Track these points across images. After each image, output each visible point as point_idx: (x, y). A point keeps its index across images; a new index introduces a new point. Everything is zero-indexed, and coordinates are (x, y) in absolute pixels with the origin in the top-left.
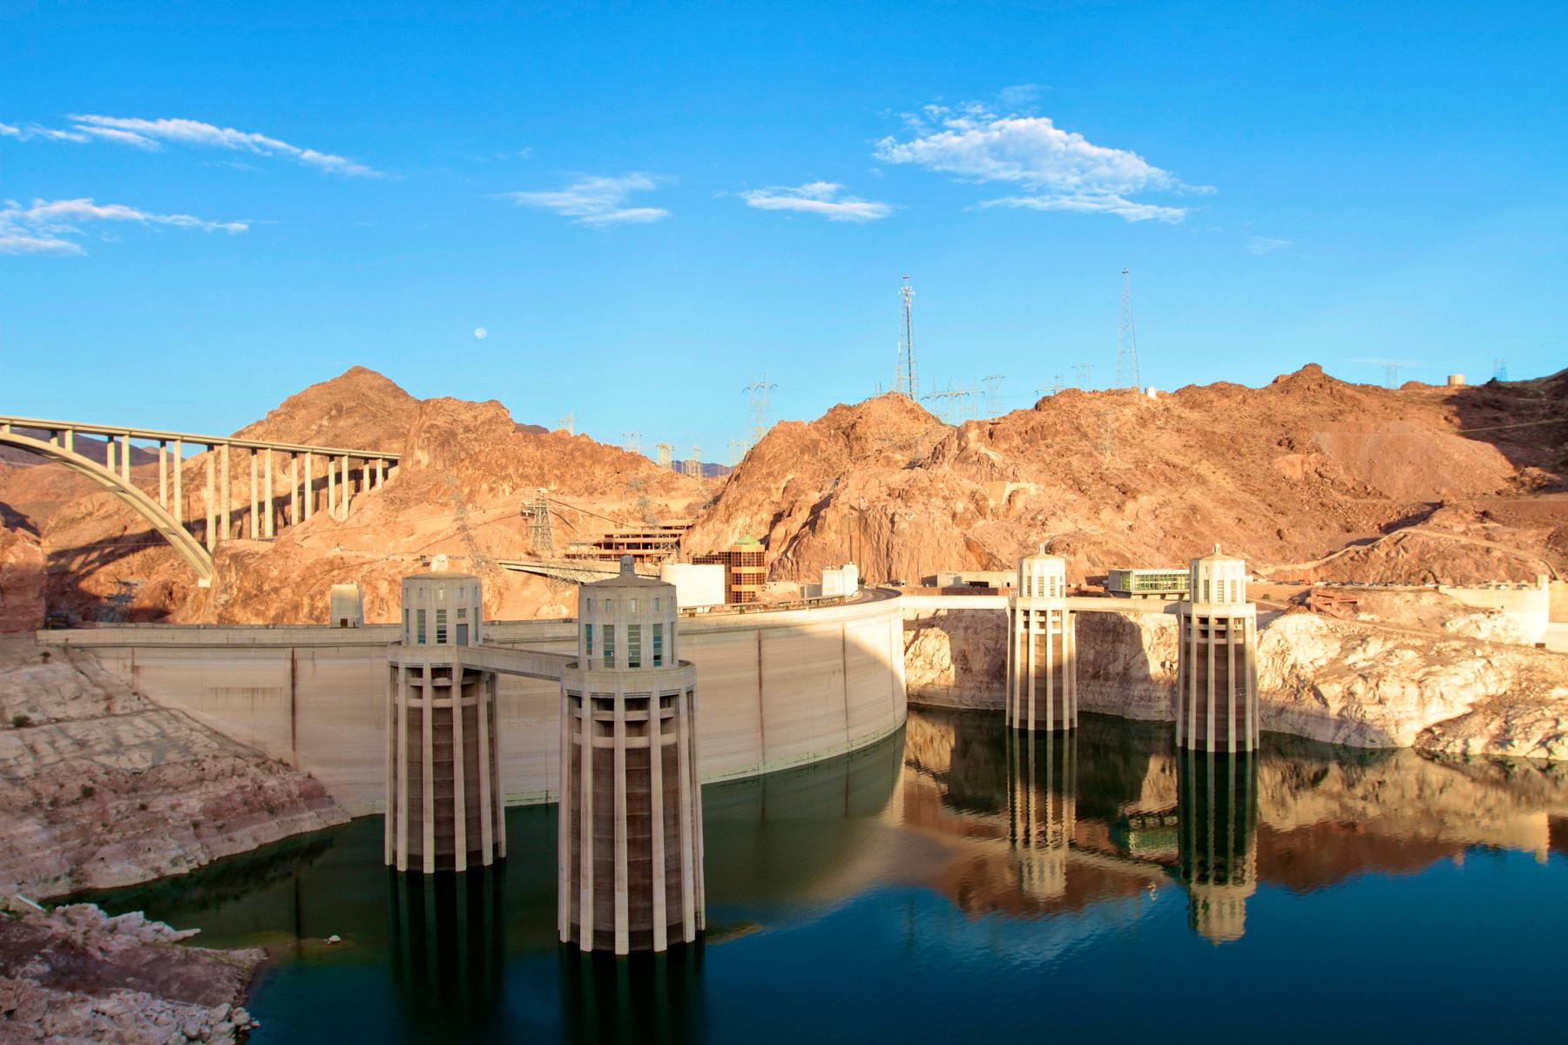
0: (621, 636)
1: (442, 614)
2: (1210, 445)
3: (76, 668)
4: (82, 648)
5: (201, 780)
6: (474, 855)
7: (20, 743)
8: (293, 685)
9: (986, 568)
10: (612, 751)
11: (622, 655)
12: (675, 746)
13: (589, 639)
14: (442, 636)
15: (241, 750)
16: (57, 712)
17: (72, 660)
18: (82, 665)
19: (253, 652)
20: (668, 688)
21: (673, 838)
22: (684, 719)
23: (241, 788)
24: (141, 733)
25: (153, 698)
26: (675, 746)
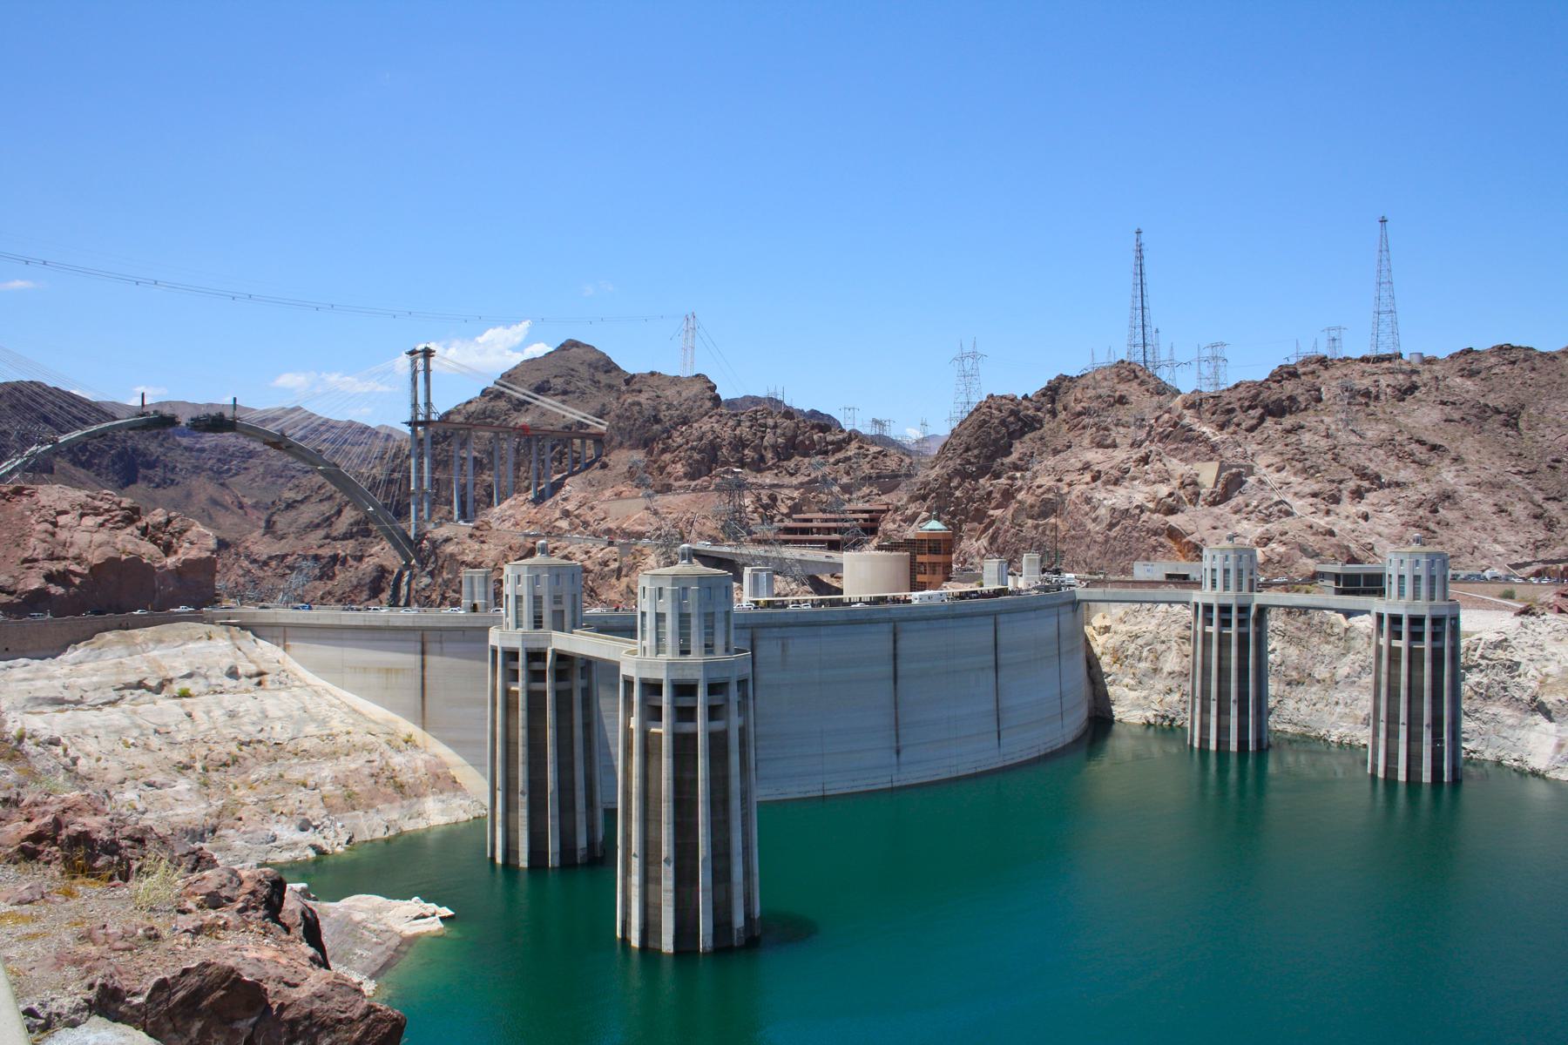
7: (181, 711)
17: (232, 638)
22: (734, 707)
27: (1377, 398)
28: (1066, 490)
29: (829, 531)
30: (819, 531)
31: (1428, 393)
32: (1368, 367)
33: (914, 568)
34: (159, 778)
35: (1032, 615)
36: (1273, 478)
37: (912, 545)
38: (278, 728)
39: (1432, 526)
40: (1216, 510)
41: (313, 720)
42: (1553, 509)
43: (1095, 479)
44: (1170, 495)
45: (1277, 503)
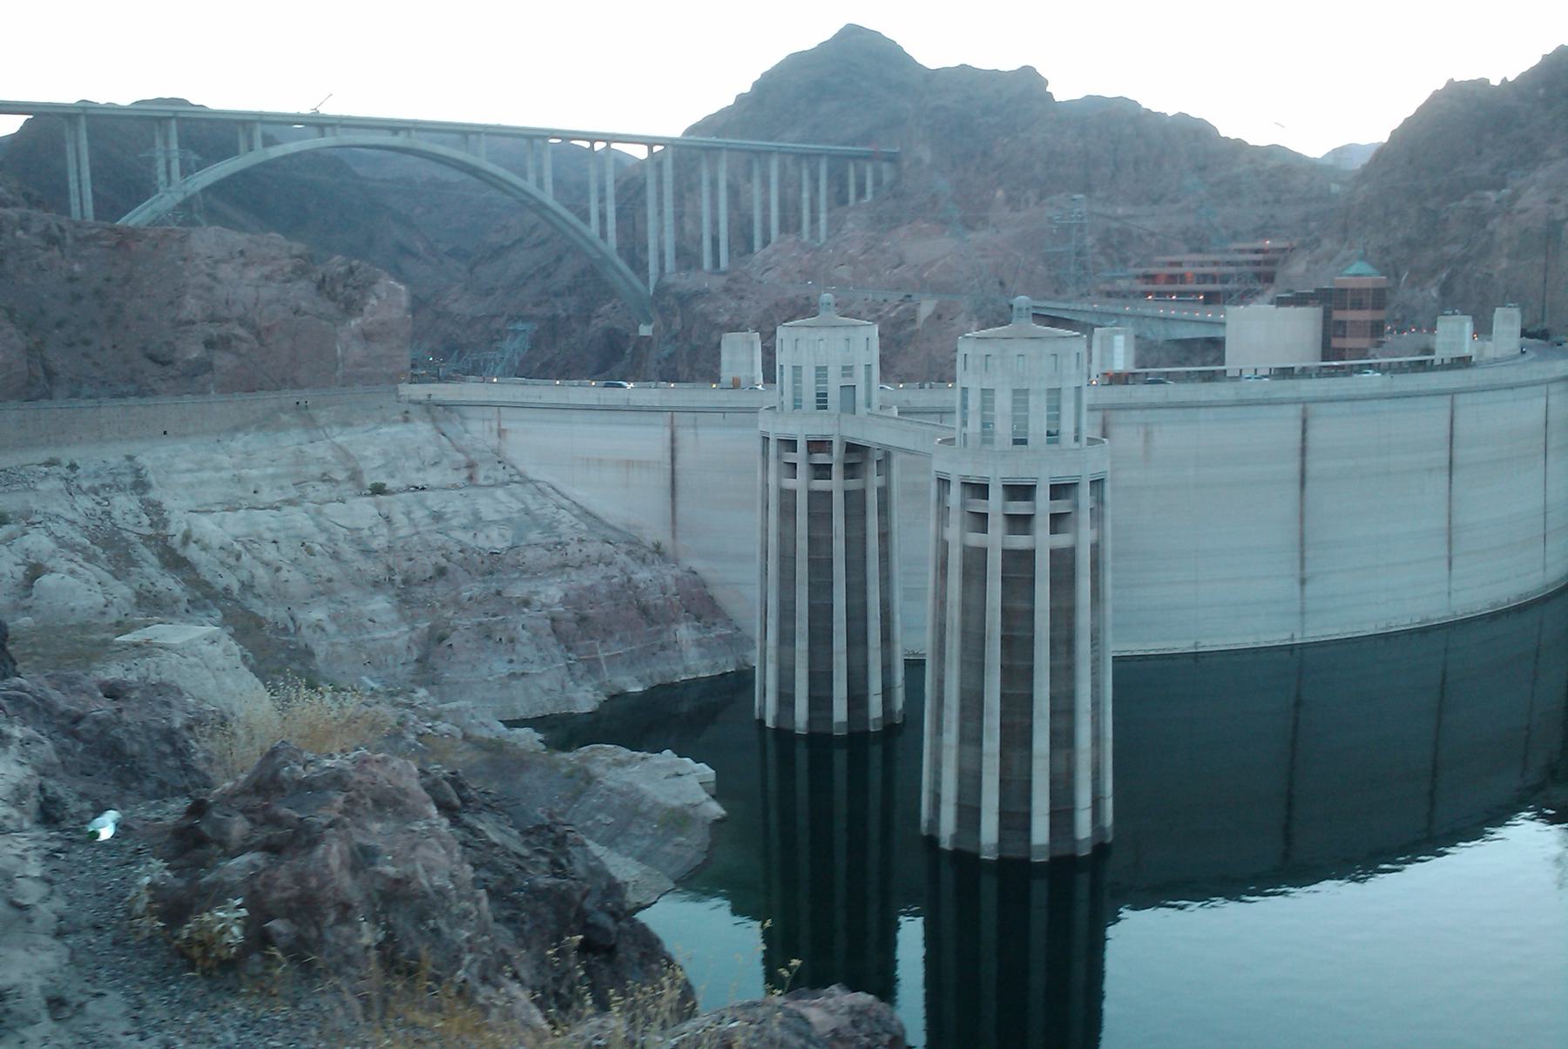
0: (1003, 402)
1: (821, 372)
3: (437, 428)
4: (446, 406)
5: (565, 566)
8: (673, 459)
11: (1003, 429)
13: (965, 406)
14: (822, 401)
15: (610, 533)
16: (418, 479)
17: (434, 420)
18: (444, 426)
20: (1062, 473)
22: (1085, 517)
23: (607, 578)
24: (502, 508)
25: (521, 468)
29: (1203, 278)
33: (1331, 330)
35: (1508, 394)
37: (1328, 298)
41: (539, 526)
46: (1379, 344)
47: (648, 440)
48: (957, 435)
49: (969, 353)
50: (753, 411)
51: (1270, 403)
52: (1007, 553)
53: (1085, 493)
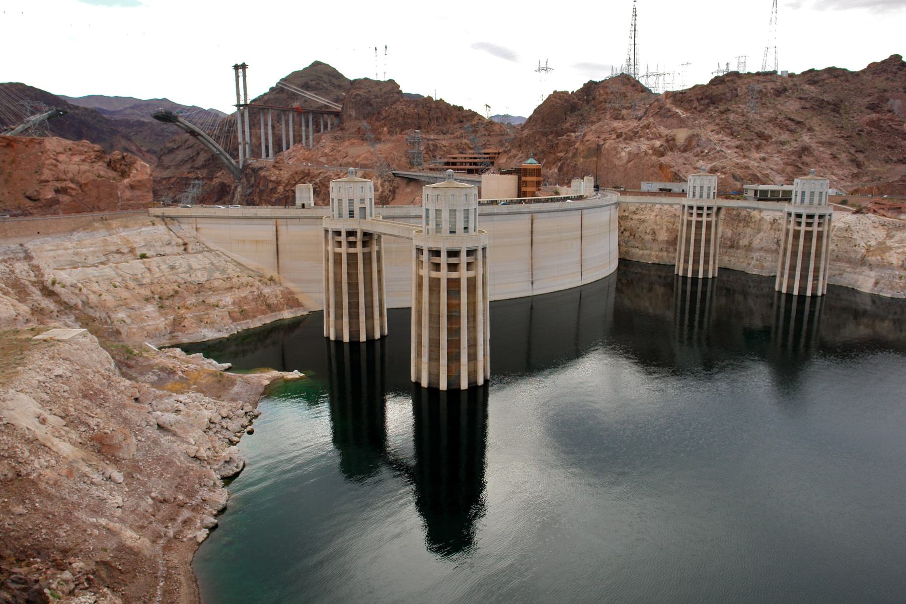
0: (445, 215)
1: (351, 201)
2: (819, 106)
6: (370, 331)
9: (670, 181)
10: (439, 279)
11: (446, 227)
12: (475, 278)
13: (427, 217)
14: (351, 214)
15: (251, 273)
16: (162, 250)
17: (166, 224)
18: (170, 227)
19: (256, 221)
20: (471, 245)
21: (472, 328)
22: (480, 263)
25: (207, 244)
26: (475, 278)
27: (766, 94)
28: (602, 143)
30: (462, 163)
31: (793, 93)
32: (760, 78)
33: (520, 184)
34: (136, 305)
36: (715, 137)
38: (199, 274)
39: (800, 165)
40: (685, 155)
42: (860, 157)
43: (618, 137)
44: (661, 146)
45: (718, 152)
46: (539, 190)
47: (266, 231)
48: (423, 229)
49: (430, 193)
50: (321, 218)
51: (520, 213)
52: (448, 280)
53: (480, 253)
